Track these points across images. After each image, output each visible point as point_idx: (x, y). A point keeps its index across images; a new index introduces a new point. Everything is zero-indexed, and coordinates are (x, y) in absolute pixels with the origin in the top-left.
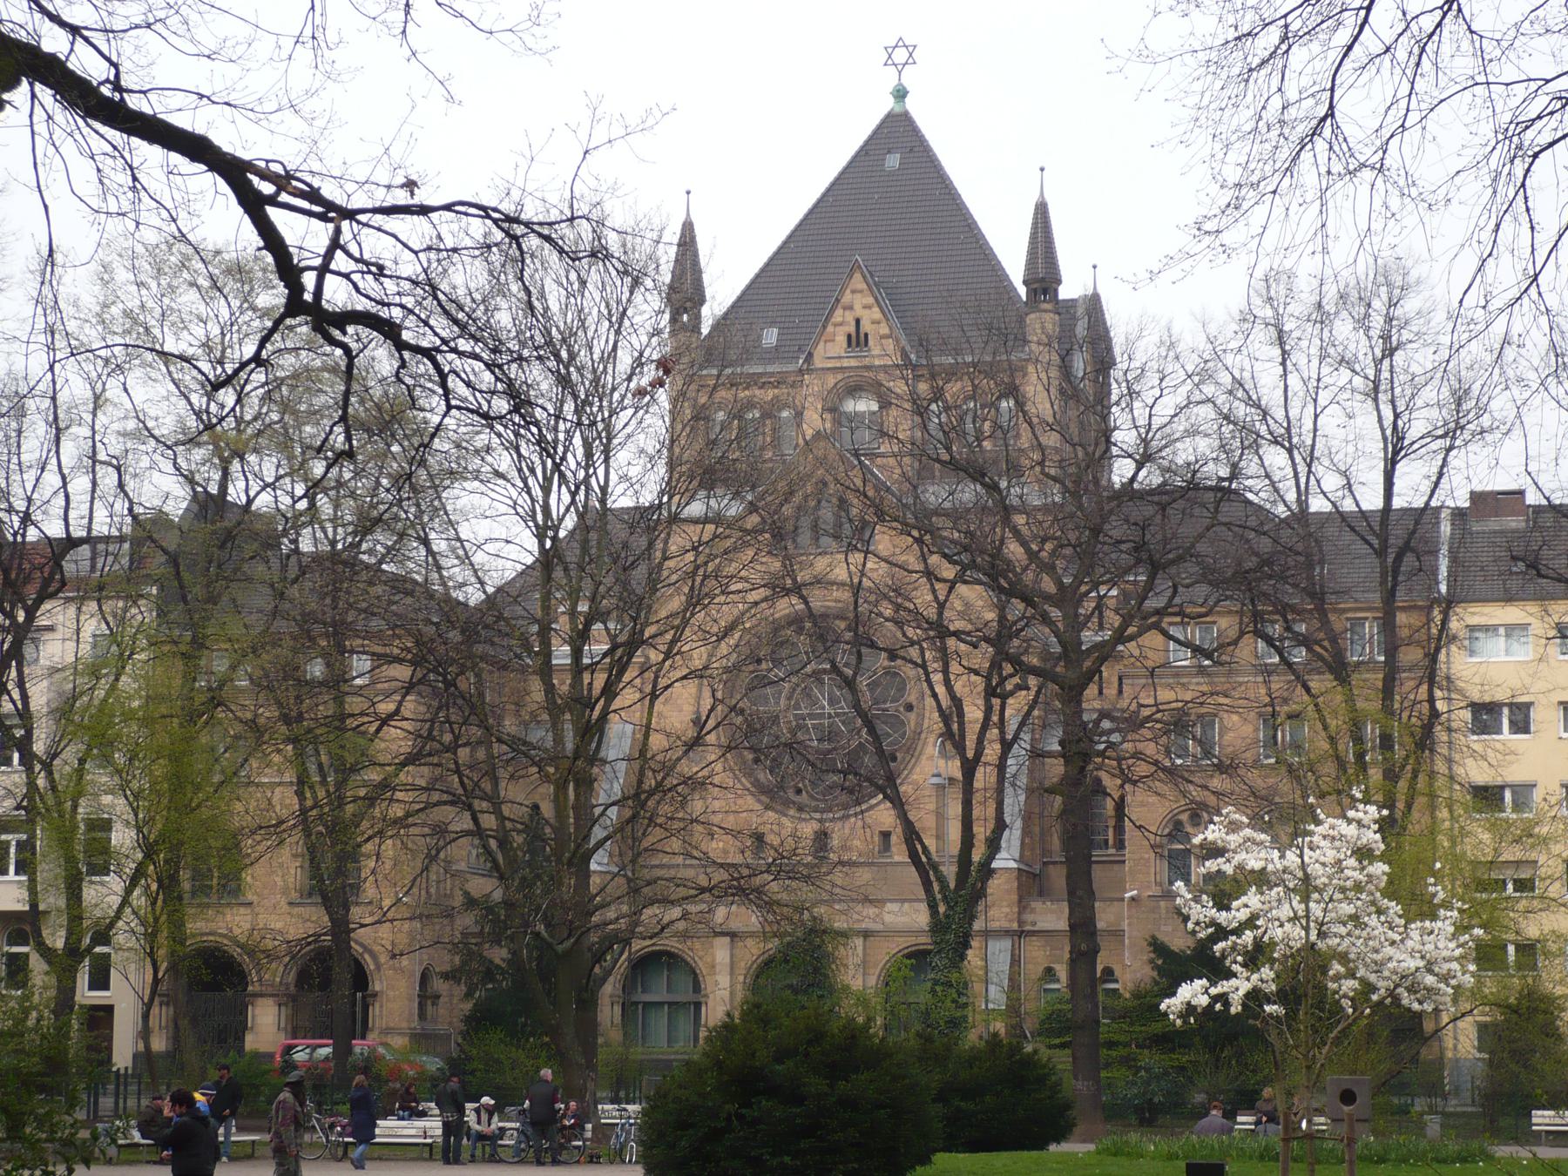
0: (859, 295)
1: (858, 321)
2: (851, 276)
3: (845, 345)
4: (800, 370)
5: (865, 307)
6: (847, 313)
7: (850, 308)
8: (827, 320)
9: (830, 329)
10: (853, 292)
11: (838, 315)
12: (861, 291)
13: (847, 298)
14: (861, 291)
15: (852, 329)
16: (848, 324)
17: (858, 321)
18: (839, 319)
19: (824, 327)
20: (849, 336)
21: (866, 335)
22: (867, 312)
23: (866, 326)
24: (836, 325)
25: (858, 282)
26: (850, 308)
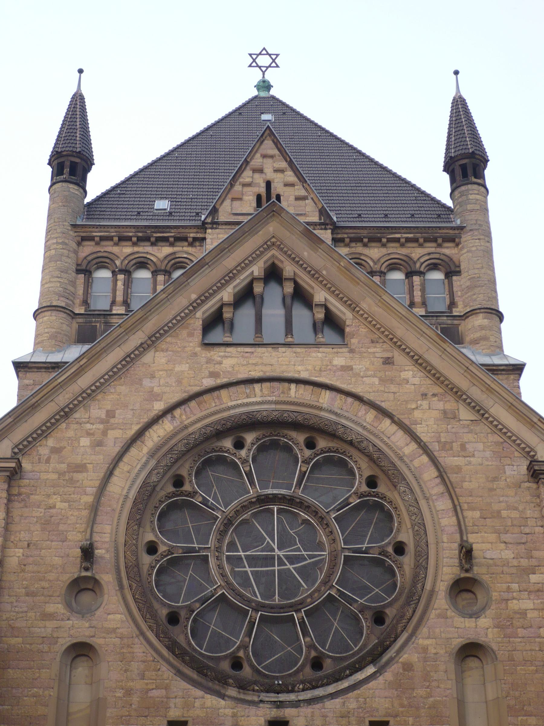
0: (270, 161)
1: (268, 184)
2: (261, 140)
3: (254, 204)
4: (204, 223)
5: (276, 171)
6: (257, 176)
7: (260, 171)
8: (235, 179)
9: (238, 188)
10: (264, 156)
11: (247, 176)
12: (272, 157)
13: (257, 161)
14: (272, 157)
15: (262, 190)
16: (258, 185)
17: (268, 184)
18: (248, 180)
19: (232, 185)
20: (259, 198)
21: (278, 197)
22: (279, 175)
23: (278, 187)
24: (244, 185)
25: (268, 147)
26: (260, 171)
